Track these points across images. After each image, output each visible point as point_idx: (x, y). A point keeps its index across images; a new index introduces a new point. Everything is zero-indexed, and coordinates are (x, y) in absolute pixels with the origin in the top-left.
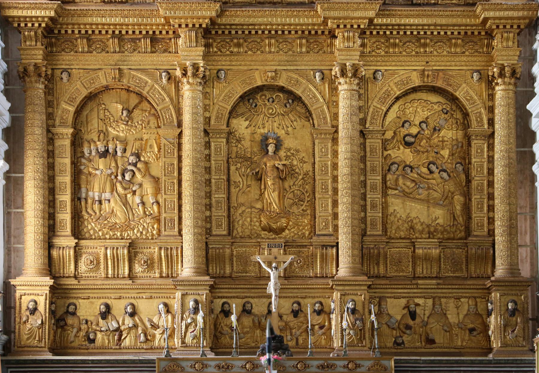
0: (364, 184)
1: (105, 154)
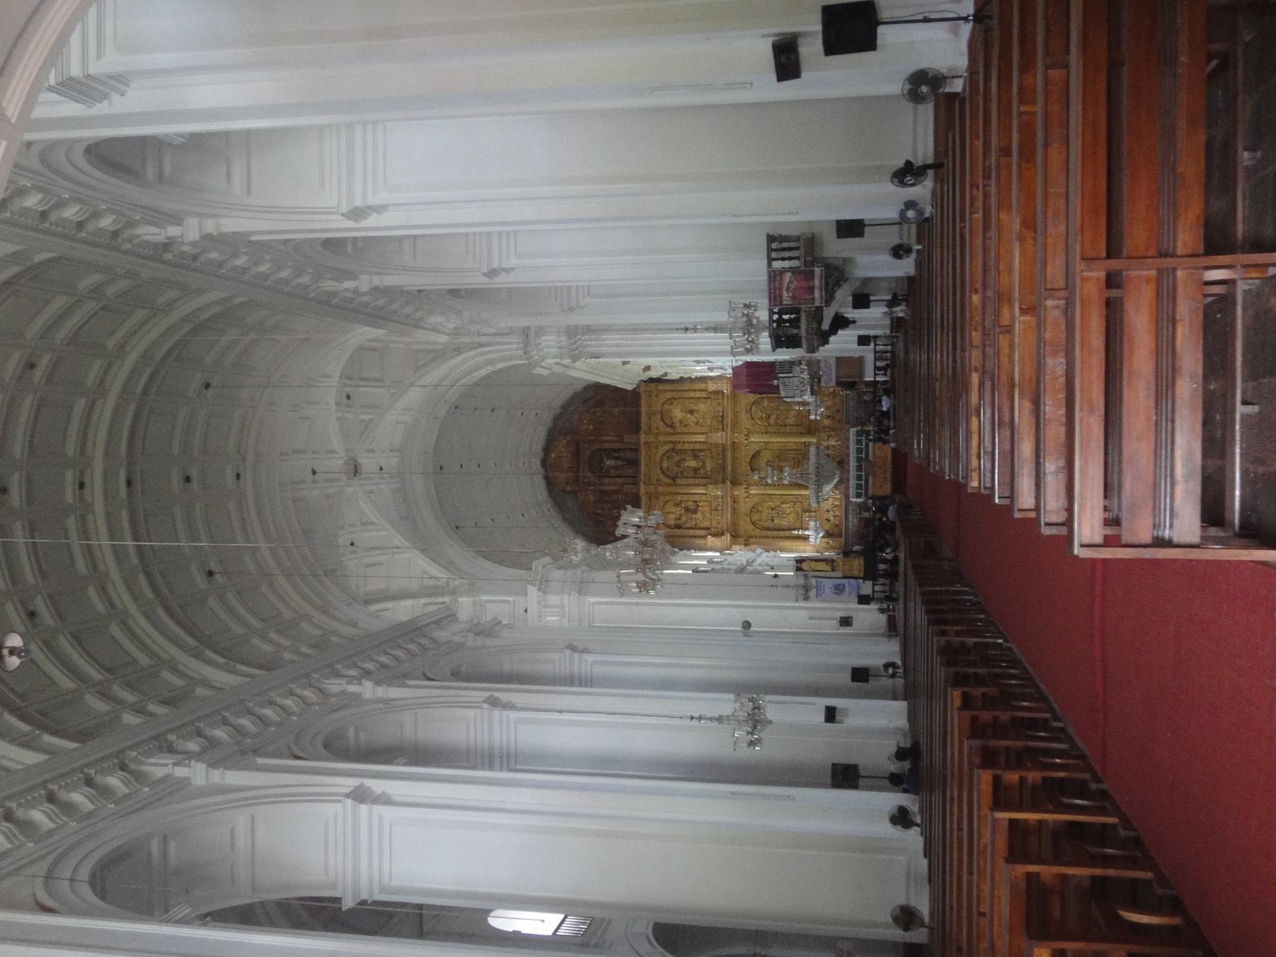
0: (784, 433)
1: (773, 520)
